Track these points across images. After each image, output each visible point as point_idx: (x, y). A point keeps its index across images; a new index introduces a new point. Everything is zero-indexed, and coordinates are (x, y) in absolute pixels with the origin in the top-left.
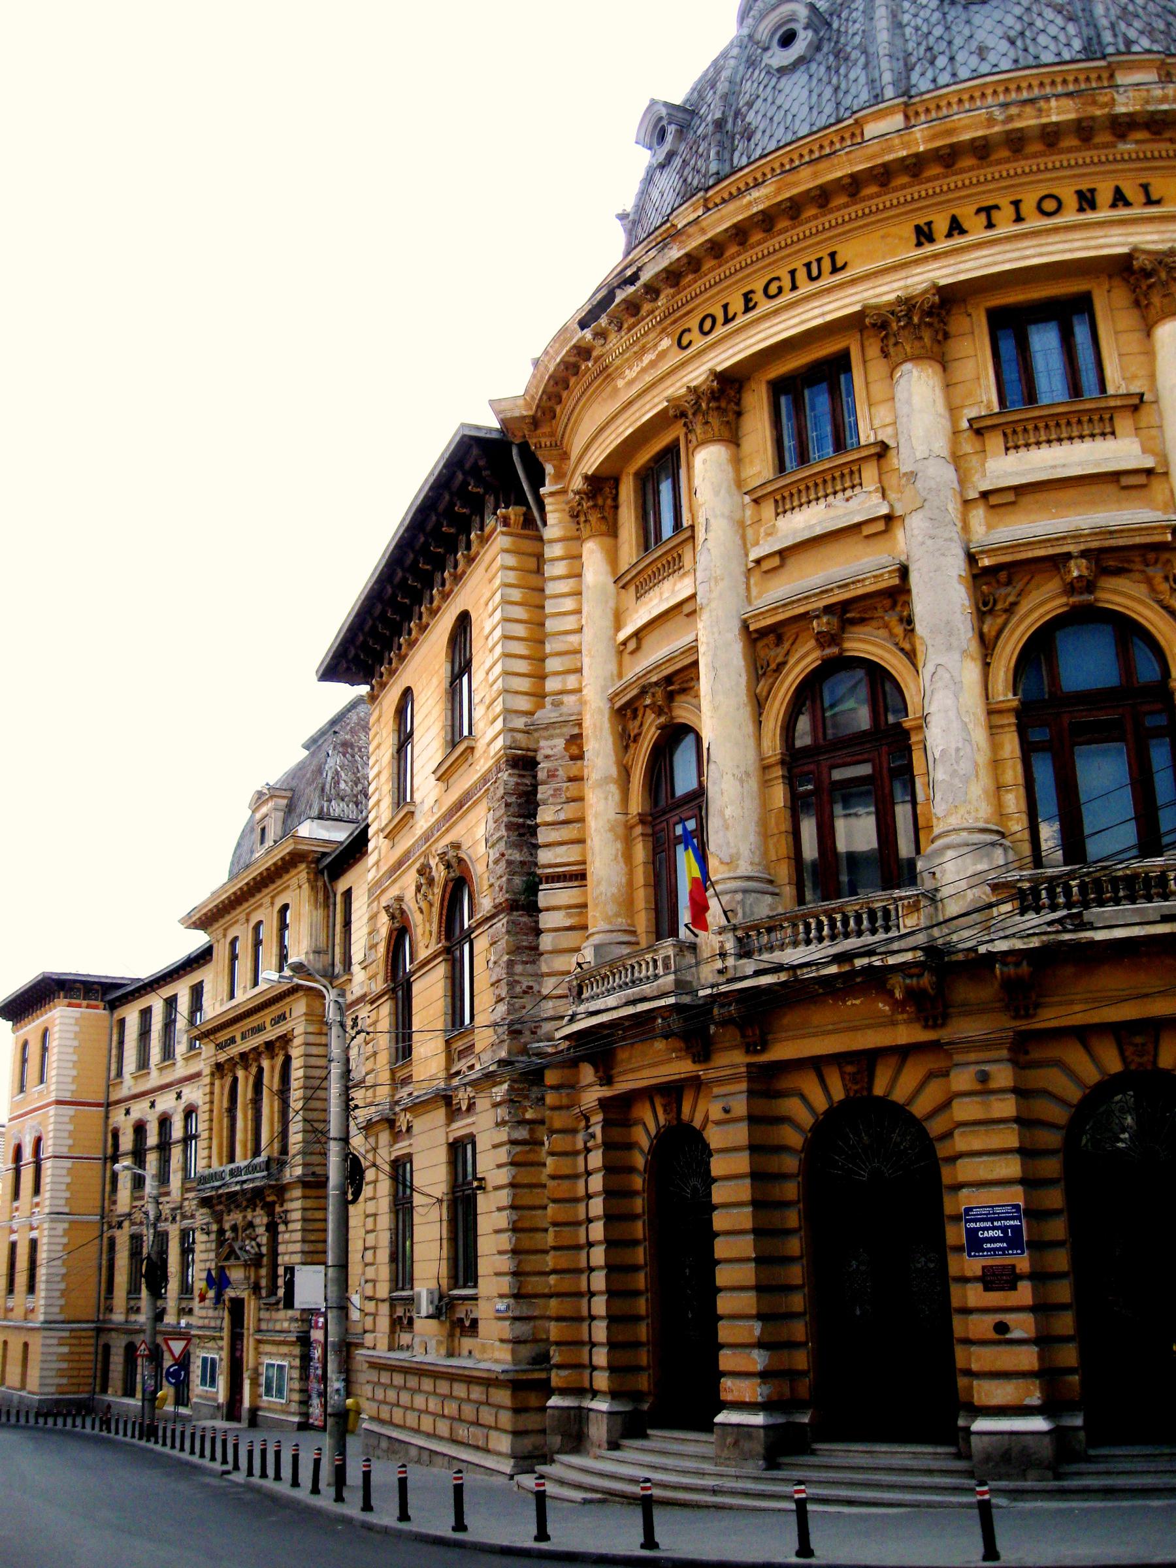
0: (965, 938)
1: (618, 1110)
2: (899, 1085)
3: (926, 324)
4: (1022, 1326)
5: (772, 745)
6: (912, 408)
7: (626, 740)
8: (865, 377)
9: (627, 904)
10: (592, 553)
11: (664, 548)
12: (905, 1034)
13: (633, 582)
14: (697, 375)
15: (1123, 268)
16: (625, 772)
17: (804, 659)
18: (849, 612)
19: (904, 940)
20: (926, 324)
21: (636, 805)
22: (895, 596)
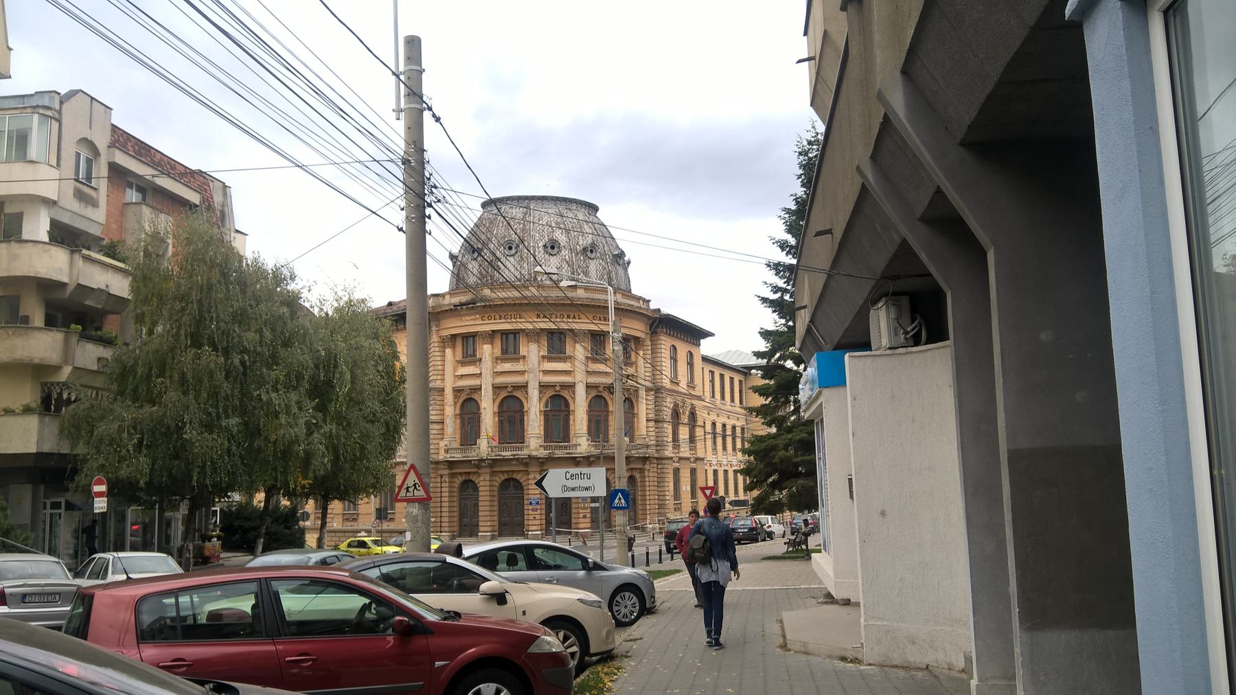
0: (534, 453)
1: (452, 475)
2: (518, 477)
3: (534, 335)
4: (538, 517)
5: (496, 410)
6: (532, 352)
7: (456, 397)
8: (522, 341)
9: (454, 432)
10: (448, 351)
11: (470, 357)
12: (521, 468)
13: (463, 363)
14: (488, 328)
15: (571, 330)
16: (455, 403)
17: (504, 394)
18: (517, 387)
19: (524, 453)
20: (534, 335)
21: (458, 412)
22: (524, 387)
